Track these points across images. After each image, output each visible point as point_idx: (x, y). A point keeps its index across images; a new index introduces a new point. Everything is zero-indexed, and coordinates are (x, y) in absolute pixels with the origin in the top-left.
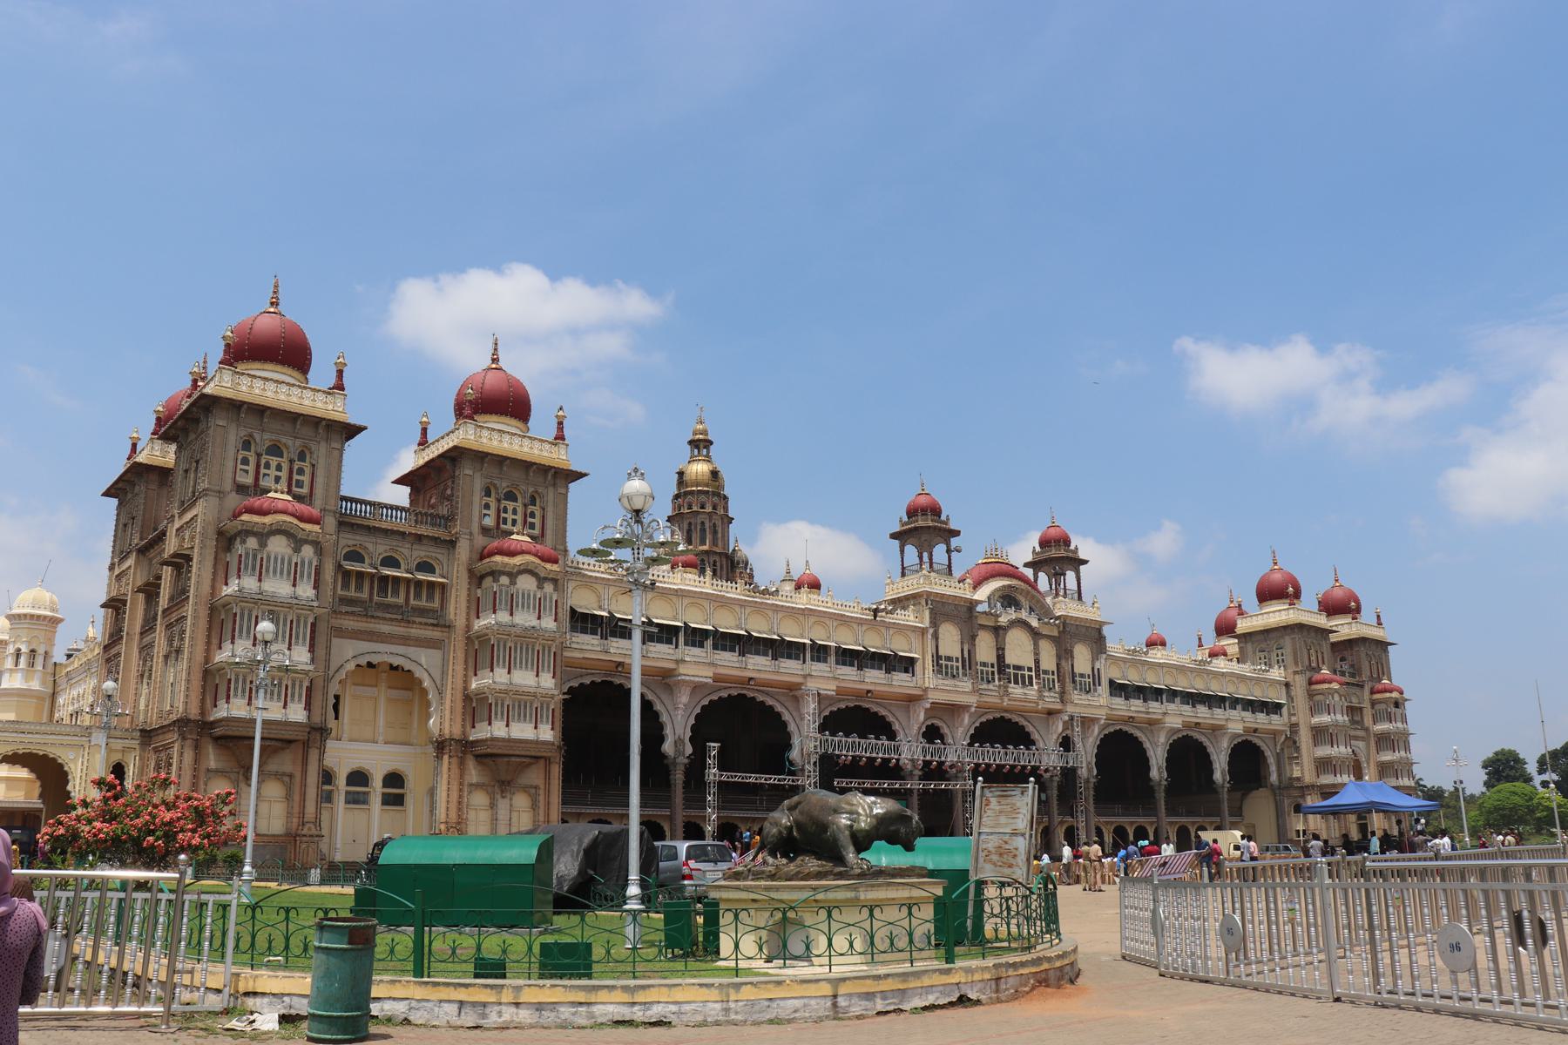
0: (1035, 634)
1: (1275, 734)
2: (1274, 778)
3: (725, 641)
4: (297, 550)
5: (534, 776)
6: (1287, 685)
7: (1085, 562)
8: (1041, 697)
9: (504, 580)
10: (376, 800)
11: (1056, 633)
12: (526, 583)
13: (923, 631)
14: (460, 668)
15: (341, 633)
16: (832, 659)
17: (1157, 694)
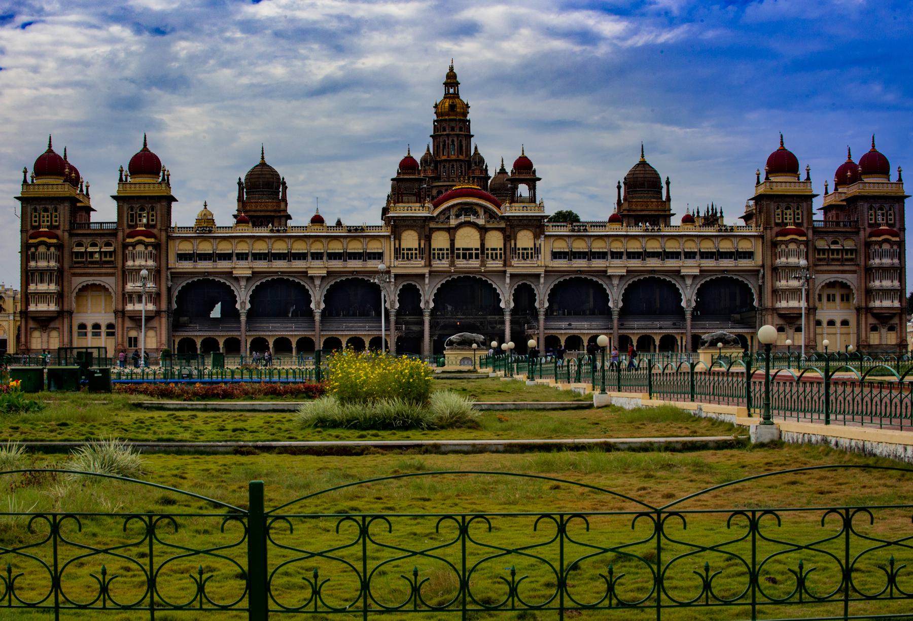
0: (483, 230)
1: (755, 273)
2: (755, 303)
3: (257, 256)
4: (48, 249)
5: (155, 323)
6: (762, 237)
7: (539, 179)
8: (483, 264)
9: (130, 248)
10: (90, 335)
11: (503, 225)
12: (140, 248)
13: (389, 237)
14: (120, 283)
15: (75, 275)
16: (325, 258)
17: (602, 255)
